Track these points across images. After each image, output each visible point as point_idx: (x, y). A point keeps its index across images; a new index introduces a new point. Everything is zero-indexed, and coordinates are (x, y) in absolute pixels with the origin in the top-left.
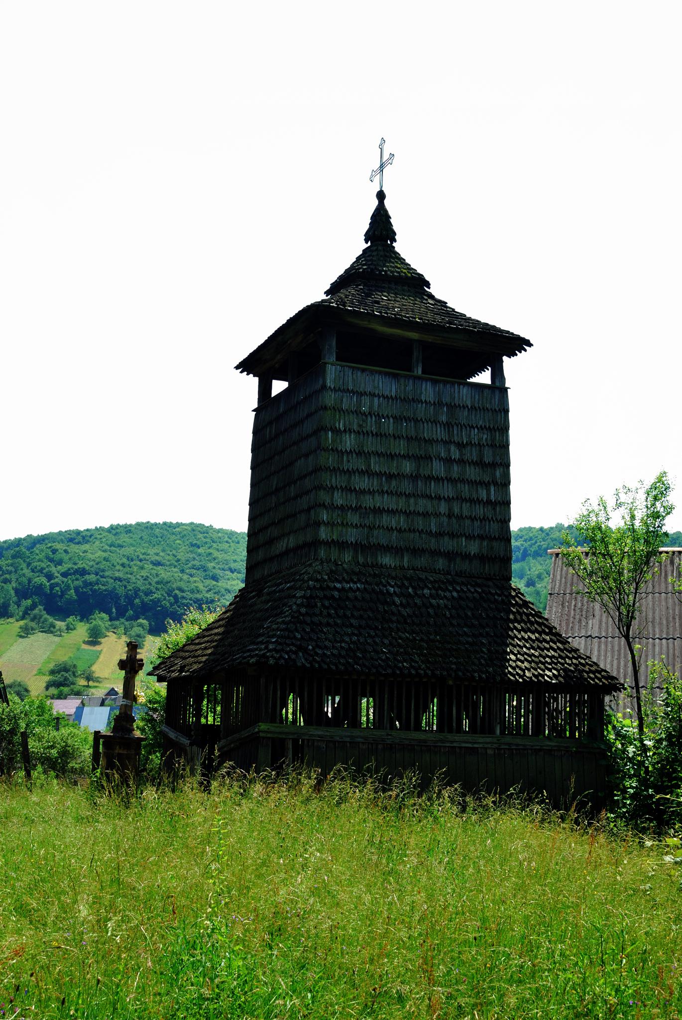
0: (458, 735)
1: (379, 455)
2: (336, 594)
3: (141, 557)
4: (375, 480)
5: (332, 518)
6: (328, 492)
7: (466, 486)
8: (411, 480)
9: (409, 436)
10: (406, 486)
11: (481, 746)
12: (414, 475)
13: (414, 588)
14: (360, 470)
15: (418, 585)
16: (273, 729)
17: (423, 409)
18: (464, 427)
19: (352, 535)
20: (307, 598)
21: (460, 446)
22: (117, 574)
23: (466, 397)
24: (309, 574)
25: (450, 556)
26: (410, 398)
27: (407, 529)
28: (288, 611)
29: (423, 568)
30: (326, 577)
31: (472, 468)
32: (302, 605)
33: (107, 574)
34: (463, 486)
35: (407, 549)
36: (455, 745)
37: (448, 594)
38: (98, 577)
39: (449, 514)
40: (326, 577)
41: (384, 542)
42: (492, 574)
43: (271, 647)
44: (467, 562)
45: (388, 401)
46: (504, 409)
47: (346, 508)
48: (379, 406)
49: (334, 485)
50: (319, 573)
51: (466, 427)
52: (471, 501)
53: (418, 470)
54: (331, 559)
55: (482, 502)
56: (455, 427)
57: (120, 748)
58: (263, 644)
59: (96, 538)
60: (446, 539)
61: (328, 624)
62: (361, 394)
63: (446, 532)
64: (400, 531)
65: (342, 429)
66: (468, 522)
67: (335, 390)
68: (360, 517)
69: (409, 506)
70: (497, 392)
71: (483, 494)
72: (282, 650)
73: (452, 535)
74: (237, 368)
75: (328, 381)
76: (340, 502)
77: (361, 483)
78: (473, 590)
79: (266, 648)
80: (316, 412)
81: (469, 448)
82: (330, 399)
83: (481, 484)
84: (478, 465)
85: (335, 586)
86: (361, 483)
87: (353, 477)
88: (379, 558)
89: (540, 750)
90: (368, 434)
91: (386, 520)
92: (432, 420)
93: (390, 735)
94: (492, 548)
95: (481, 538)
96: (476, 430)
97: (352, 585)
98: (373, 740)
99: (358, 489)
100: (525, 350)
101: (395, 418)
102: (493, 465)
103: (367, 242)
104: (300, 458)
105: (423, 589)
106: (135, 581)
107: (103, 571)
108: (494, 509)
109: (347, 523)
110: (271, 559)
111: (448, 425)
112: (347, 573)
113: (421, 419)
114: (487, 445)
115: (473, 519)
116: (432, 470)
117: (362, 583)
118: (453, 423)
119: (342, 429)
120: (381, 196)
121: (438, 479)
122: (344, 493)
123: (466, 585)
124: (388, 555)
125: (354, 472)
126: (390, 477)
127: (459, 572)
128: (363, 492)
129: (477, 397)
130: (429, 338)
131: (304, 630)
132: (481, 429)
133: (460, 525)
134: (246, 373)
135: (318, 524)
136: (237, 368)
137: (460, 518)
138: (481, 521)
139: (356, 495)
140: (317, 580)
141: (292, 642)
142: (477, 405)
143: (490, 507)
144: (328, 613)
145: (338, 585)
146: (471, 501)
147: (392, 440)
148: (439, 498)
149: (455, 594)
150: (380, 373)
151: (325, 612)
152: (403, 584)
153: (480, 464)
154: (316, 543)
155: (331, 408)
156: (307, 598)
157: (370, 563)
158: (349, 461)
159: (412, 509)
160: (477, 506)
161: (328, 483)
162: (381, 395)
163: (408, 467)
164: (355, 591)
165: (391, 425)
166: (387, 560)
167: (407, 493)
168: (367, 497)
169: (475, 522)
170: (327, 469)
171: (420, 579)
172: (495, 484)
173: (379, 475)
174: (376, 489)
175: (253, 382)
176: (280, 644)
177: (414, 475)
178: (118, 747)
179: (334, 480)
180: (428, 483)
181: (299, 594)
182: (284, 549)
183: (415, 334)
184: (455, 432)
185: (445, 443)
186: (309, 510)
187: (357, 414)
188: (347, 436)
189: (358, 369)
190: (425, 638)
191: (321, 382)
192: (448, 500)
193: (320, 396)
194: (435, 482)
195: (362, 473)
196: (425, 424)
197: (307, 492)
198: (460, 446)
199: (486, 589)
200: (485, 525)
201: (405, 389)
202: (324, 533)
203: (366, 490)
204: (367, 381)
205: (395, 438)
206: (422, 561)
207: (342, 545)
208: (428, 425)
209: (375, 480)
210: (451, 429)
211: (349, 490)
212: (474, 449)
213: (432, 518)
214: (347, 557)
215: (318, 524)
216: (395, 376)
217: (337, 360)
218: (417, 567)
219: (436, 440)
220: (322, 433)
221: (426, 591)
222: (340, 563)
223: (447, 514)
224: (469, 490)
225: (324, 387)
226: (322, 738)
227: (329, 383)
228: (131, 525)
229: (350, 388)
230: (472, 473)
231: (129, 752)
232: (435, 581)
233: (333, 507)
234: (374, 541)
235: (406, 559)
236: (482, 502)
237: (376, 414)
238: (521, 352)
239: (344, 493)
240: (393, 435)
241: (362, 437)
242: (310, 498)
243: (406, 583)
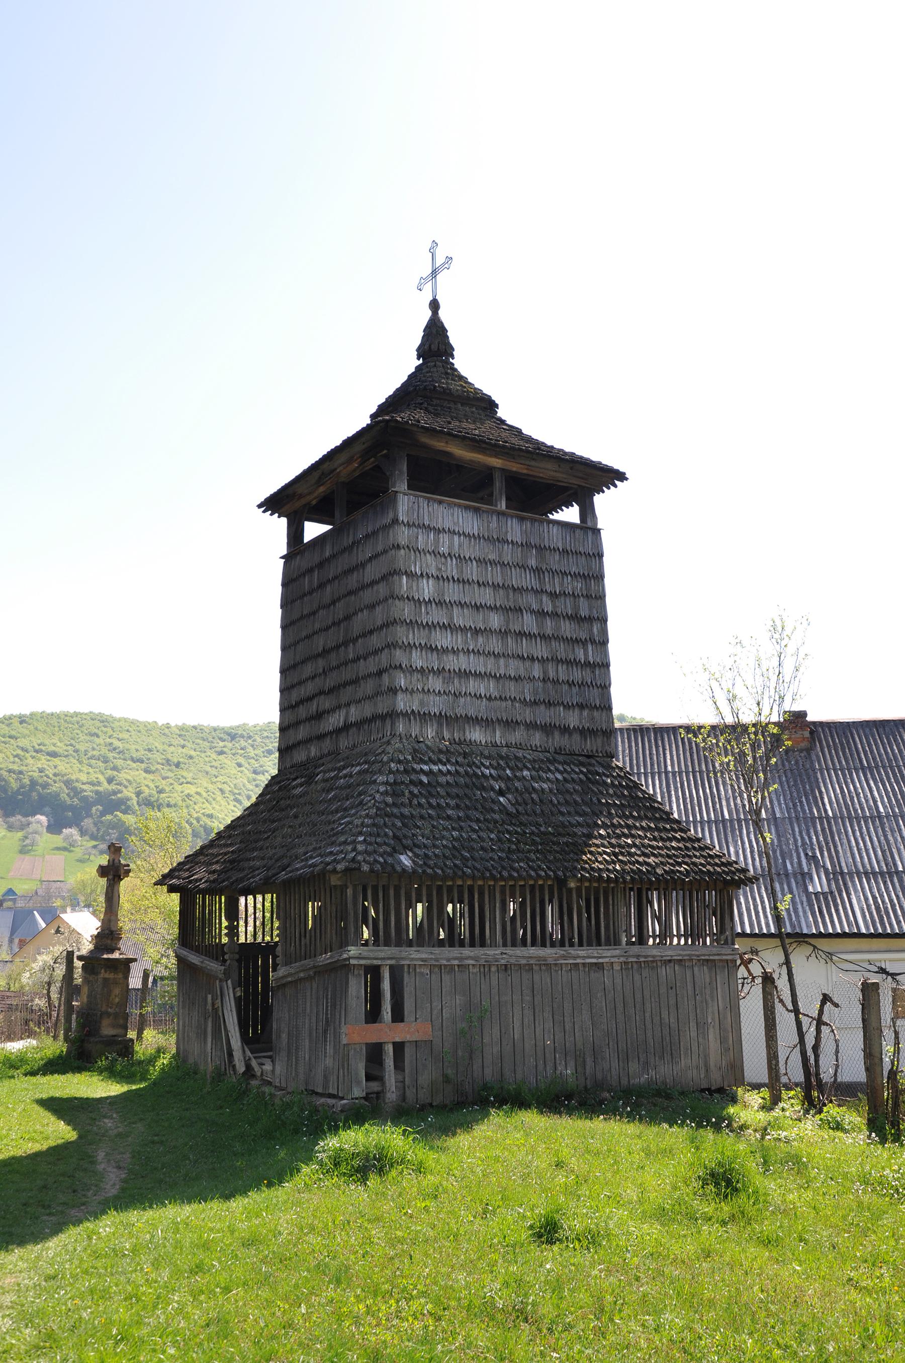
0: (581, 948)
1: (461, 605)
2: (425, 779)
3: (37, 747)
4: (459, 637)
5: (411, 682)
6: (405, 650)
7: (562, 644)
8: (500, 637)
9: (496, 583)
10: (495, 645)
11: (607, 960)
12: (503, 630)
13: (511, 769)
14: (441, 624)
15: (516, 766)
16: (365, 954)
17: (510, 551)
18: (555, 573)
19: (436, 705)
20: (391, 785)
21: (553, 596)
23: (557, 539)
24: (389, 753)
25: (547, 729)
26: (495, 537)
27: (498, 697)
28: (370, 801)
29: (518, 744)
30: (410, 758)
31: (567, 622)
32: (386, 793)
34: (557, 644)
35: (499, 721)
36: (578, 961)
37: (550, 775)
39: (544, 679)
40: (410, 758)
41: (472, 712)
42: (594, 751)
43: (360, 848)
44: (567, 736)
45: (470, 540)
46: (598, 554)
47: (427, 671)
48: (460, 546)
49: (412, 643)
50: (401, 752)
51: (558, 574)
52: (569, 663)
53: (508, 625)
54: (411, 735)
55: (580, 664)
56: (546, 574)
57: (106, 972)
58: (349, 844)
60: (542, 707)
61: (422, 817)
62: (438, 531)
63: (542, 700)
64: (490, 699)
65: (419, 573)
66: (565, 687)
68: (444, 682)
69: (499, 668)
70: (590, 533)
71: (580, 655)
72: (375, 852)
73: (549, 704)
74: (259, 506)
75: (400, 514)
76: (419, 663)
77: (443, 640)
78: (577, 770)
79: (354, 849)
80: (385, 552)
81: (563, 598)
82: (403, 535)
83: (578, 642)
84: (573, 619)
85: (421, 768)
86: (443, 640)
87: (433, 633)
88: (467, 733)
89: (670, 961)
90: (449, 580)
91: (473, 686)
92: (520, 565)
93: (505, 954)
94: (593, 718)
95: (581, 707)
96: (569, 577)
97: (441, 767)
98: (486, 961)
99: (439, 648)
100: (616, 486)
101: (479, 561)
102: (590, 619)
103: (418, 359)
104: (361, 610)
105: (522, 770)
108: (593, 672)
109: (429, 690)
110: (321, 737)
111: (538, 571)
112: (433, 752)
113: (508, 563)
114: (582, 595)
115: (571, 684)
116: (523, 625)
117: (452, 764)
118: (544, 569)
119: (419, 573)
120: (435, 305)
121: (530, 636)
122: (424, 652)
123: (568, 765)
124: (477, 728)
125: (435, 627)
126: (477, 632)
127: (558, 748)
128: (445, 651)
129: (568, 538)
130: (514, 467)
131: (394, 825)
132: (575, 576)
133: (556, 692)
134: (270, 512)
136: (259, 506)
137: (556, 682)
138: (579, 687)
139: (438, 654)
140: (400, 762)
141: (385, 842)
142: (569, 549)
143: (588, 669)
144: (419, 803)
145: (425, 768)
146: (569, 663)
147: (476, 586)
148: (532, 659)
149: (559, 777)
150: (459, 506)
151: (415, 802)
152: (499, 764)
153: (575, 618)
154: (392, 715)
155: (405, 547)
156: (391, 785)
157: (457, 740)
158: (428, 613)
159: (502, 672)
160: (575, 668)
161: (405, 641)
162: (461, 532)
163: (495, 621)
164: (445, 775)
165: (475, 569)
166: (476, 735)
167: (496, 653)
168: (451, 657)
169: (573, 688)
170: (403, 622)
171: (516, 758)
172: (593, 642)
173: (463, 630)
174: (460, 649)
175: (279, 525)
176: (370, 844)
177: (503, 630)
178: (103, 971)
179: (411, 636)
180: (519, 641)
181: (381, 779)
182: (341, 724)
183: (498, 460)
184: (547, 580)
185: (536, 592)
186: (380, 673)
187: (435, 556)
188: (425, 581)
189: (435, 500)
190: (536, 831)
191: (391, 515)
192: (543, 661)
193: (391, 532)
194: (526, 640)
195: (444, 627)
196: (513, 569)
197: (376, 652)
198: (553, 596)
199: (591, 768)
200: (584, 691)
201: (488, 526)
202: (402, 703)
203: (450, 648)
204: (445, 515)
205: (479, 585)
206: (518, 736)
207: (424, 717)
208: (516, 570)
209: (459, 637)
210: (542, 576)
211: (432, 649)
212: (568, 601)
213: (526, 683)
214: (430, 732)
215: (393, 691)
216: (476, 510)
217: (409, 489)
218: (511, 743)
219: (525, 588)
220: (396, 578)
221: (526, 773)
222: (422, 740)
223: (541, 679)
224: (565, 649)
225: (395, 521)
226: (425, 961)
229: (427, 523)
230: (567, 629)
231: (116, 976)
232: (534, 761)
233: (411, 669)
234: (460, 711)
235: (498, 733)
236: (580, 664)
237: (457, 555)
238: (609, 488)
239: (424, 652)
240: (478, 581)
241: (441, 582)
242: (380, 660)
243: (502, 762)
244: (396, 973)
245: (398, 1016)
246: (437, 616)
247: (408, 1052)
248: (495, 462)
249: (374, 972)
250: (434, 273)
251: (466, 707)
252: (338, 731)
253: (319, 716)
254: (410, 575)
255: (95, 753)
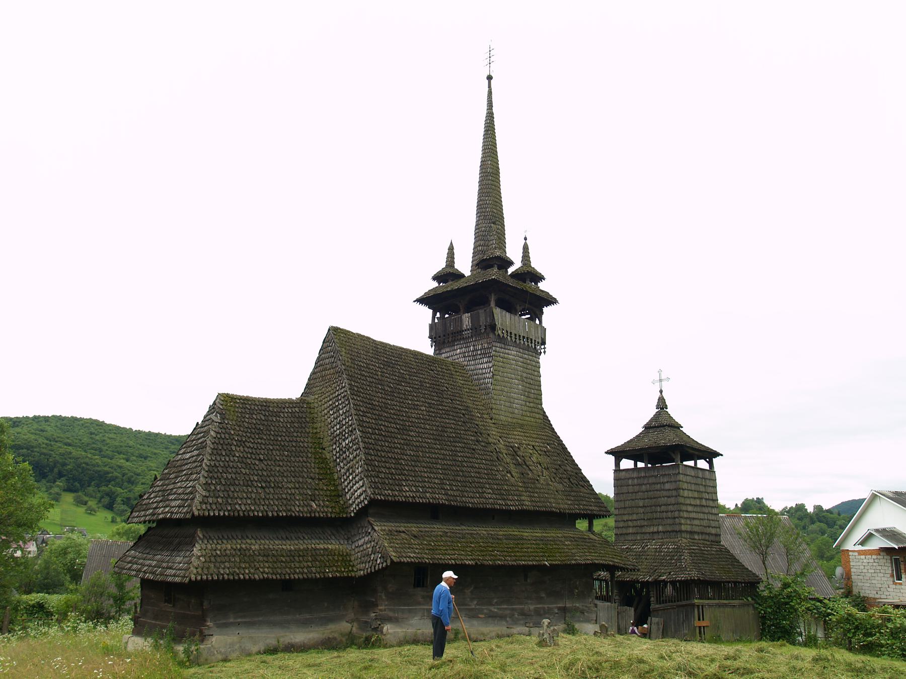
3: (57, 439)
22: (44, 451)
33: (35, 450)
38: (29, 451)
59: (24, 424)
62: (687, 475)
67: (682, 474)
76: (685, 516)
77: (690, 508)
82: (681, 477)
86: (690, 508)
106: (54, 456)
107: (33, 447)
120: (661, 392)
128: (691, 512)
135: (681, 524)
166: (696, 537)
175: (612, 458)
186: (675, 518)
225: (679, 473)
227: (681, 472)
228: (48, 417)
244: (702, 606)
245: (703, 620)
246: (688, 501)
247: (705, 628)
248: (697, 453)
249: (698, 606)
250: (661, 380)
251: (696, 529)
252: (653, 533)
253: (642, 526)
254: (683, 489)
255: (94, 446)
